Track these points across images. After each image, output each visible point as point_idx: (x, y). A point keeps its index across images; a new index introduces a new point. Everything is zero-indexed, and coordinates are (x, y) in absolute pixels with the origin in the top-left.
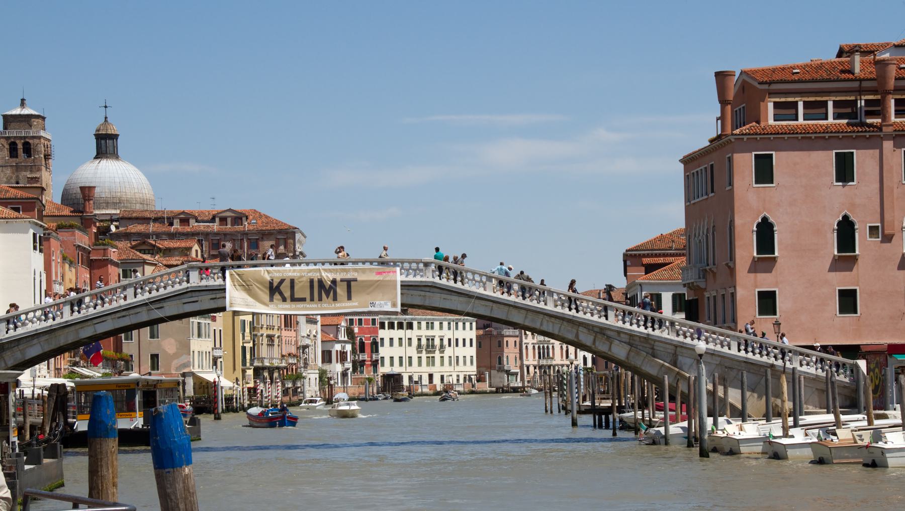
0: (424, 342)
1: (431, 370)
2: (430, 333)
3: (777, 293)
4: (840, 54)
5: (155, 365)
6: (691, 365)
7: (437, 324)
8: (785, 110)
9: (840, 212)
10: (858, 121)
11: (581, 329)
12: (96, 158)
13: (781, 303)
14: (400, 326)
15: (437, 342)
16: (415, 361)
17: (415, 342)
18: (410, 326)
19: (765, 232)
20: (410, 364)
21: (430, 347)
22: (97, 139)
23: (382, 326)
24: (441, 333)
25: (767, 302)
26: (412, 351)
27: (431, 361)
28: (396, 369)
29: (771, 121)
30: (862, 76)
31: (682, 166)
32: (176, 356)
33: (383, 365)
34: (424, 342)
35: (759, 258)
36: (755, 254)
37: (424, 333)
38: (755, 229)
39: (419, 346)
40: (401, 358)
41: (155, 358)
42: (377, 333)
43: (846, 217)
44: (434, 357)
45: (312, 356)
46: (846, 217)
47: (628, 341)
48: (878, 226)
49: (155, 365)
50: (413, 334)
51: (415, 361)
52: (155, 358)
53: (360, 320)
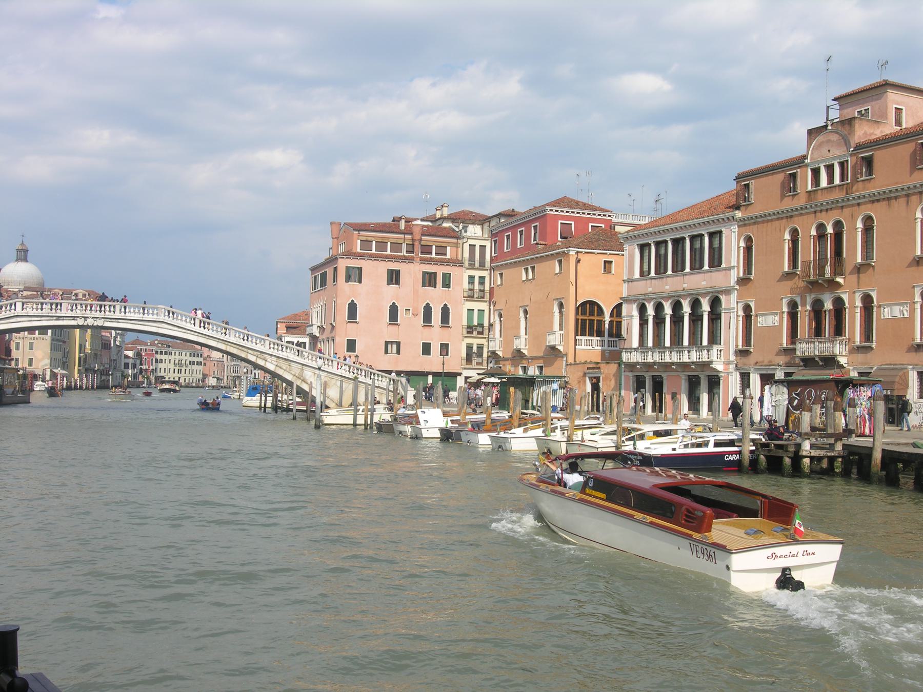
0: (177, 362)
1: (179, 375)
2: (180, 357)
3: (357, 341)
4: (394, 220)
5: (30, 364)
6: (311, 376)
7: (184, 354)
8: (366, 244)
9: (392, 300)
10: (402, 254)
11: (250, 351)
12: (17, 260)
13: (358, 346)
14: (166, 353)
15: (183, 362)
16: (172, 371)
17: (172, 362)
18: (171, 354)
19: (352, 308)
20: (169, 372)
21: (180, 364)
22: (17, 252)
23: (157, 352)
24: (186, 358)
25: (351, 346)
26: (172, 366)
27: (180, 371)
28: (162, 374)
29: (359, 250)
30: (405, 231)
31: (310, 271)
32: (43, 359)
33: (156, 372)
34: (177, 362)
35: (348, 322)
36: (347, 319)
37: (177, 357)
38: (347, 306)
39: (174, 363)
40: (165, 369)
41: (31, 360)
42: (153, 355)
43: (394, 303)
44: (181, 370)
45: (118, 365)
46: (394, 303)
47: (276, 360)
48: (409, 310)
49: (30, 364)
50: (172, 357)
51: (172, 371)
52: (31, 360)
53: (146, 349)
